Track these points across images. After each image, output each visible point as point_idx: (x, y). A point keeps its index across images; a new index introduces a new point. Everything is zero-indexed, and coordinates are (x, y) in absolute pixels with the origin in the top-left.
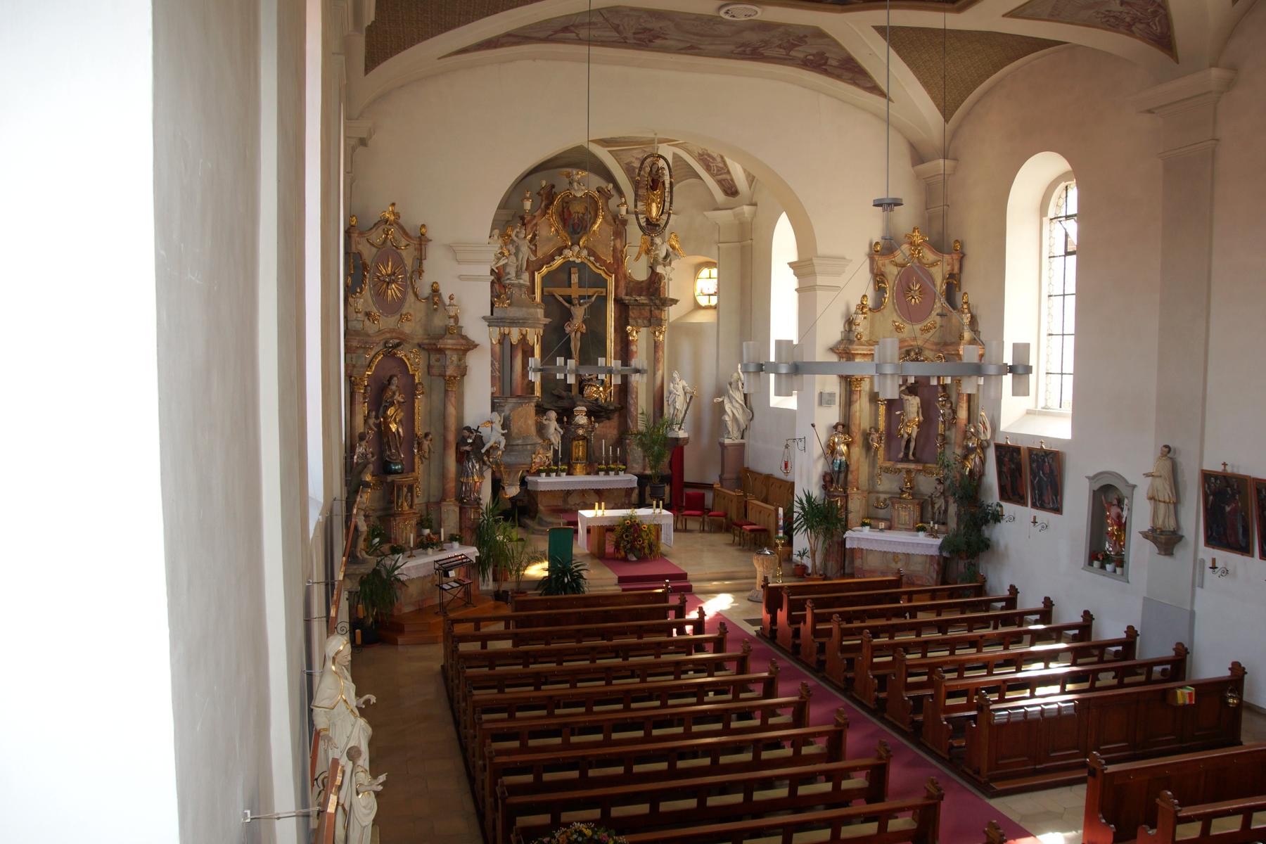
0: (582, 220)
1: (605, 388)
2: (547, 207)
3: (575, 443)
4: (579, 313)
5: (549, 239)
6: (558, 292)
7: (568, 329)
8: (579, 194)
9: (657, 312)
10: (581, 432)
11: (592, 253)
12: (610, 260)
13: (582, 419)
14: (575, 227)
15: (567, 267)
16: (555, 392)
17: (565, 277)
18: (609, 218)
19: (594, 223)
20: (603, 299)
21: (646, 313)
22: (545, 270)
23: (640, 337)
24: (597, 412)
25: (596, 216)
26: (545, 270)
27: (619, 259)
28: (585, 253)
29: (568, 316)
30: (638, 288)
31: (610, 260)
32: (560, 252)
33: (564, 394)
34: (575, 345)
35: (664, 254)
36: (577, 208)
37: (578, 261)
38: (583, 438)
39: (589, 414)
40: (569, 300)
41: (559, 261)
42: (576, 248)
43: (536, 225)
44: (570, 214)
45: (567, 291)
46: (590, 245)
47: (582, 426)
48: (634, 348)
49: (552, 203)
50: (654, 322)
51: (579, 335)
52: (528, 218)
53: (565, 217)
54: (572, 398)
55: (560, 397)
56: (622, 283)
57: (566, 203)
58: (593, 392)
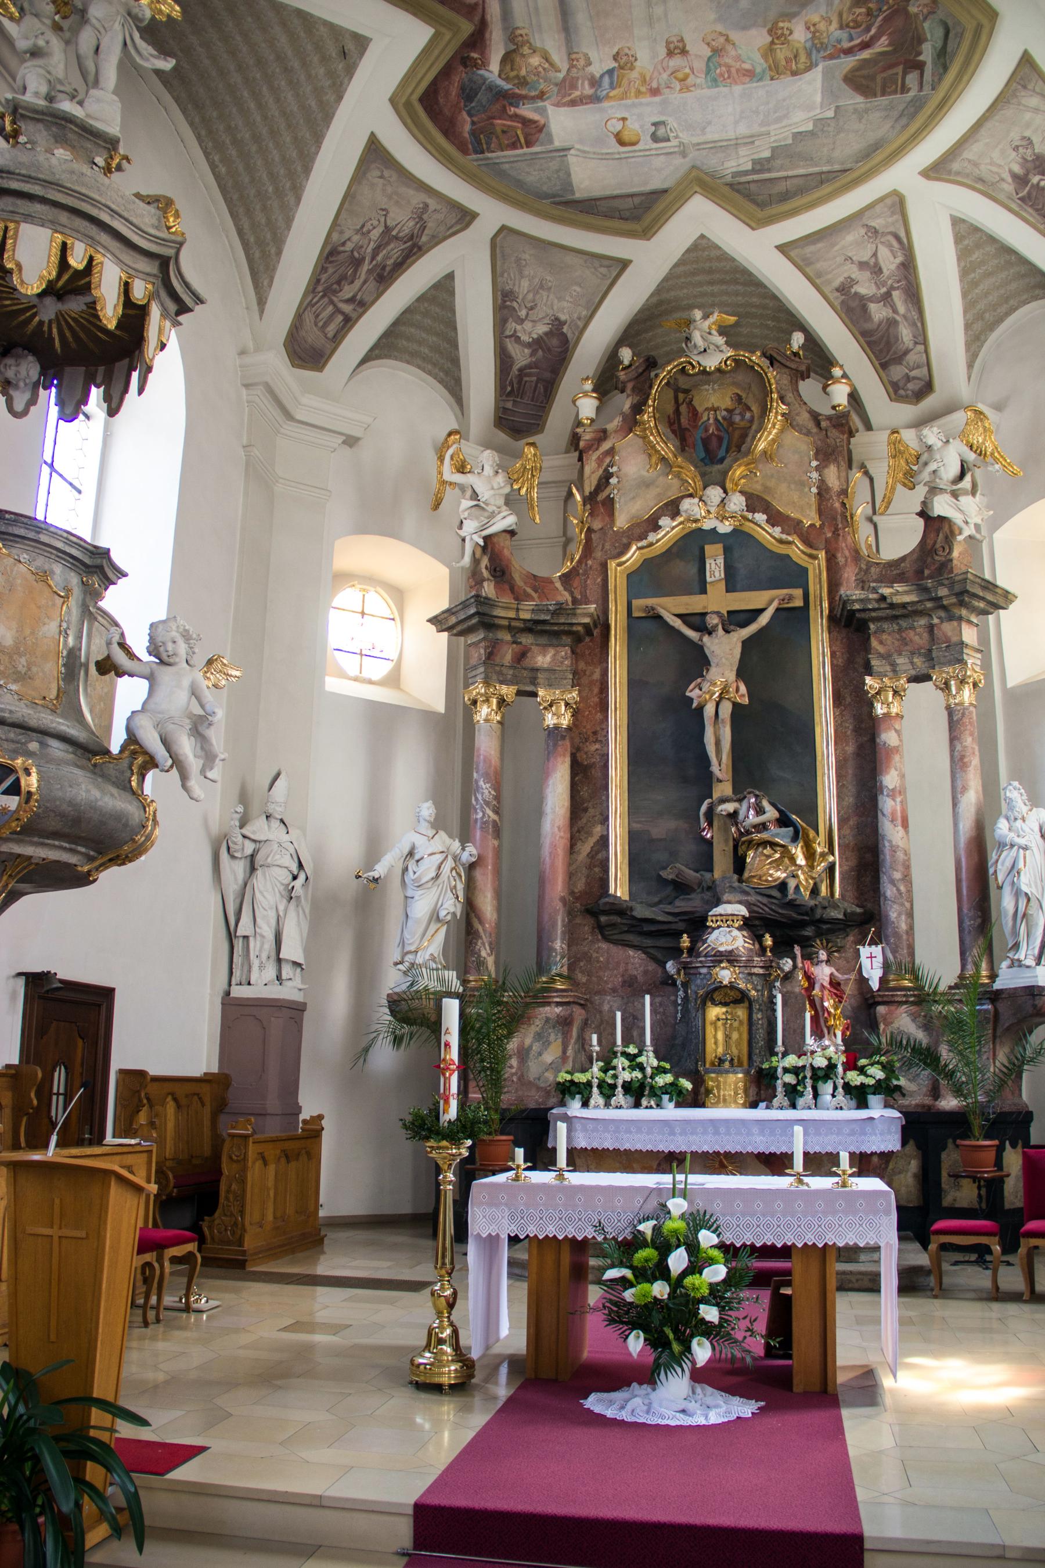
0: (727, 425)
1: (810, 855)
2: (638, 408)
3: (714, 1012)
4: (725, 650)
5: (646, 484)
6: (670, 607)
7: (693, 693)
8: (711, 362)
9: (948, 628)
10: (725, 975)
11: (755, 502)
12: (810, 518)
13: (726, 938)
14: (712, 447)
15: (695, 541)
16: (668, 874)
17: (693, 570)
18: (804, 418)
19: (761, 427)
20: (793, 619)
21: (918, 637)
22: (633, 556)
23: (914, 717)
24: (787, 926)
25: (765, 411)
26: (633, 556)
27: (834, 515)
28: (737, 502)
29: (697, 662)
30: (894, 571)
31: (810, 518)
32: (673, 508)
33: (691, 875)
34: (718, 740)
35: (954, 470)
36: (714, 400)
37: (725, 528)
38: (735, 997)
39: (752, 926)
40: (697, 621)
41: (669, 530)
42: (714, 493)
43: (611, 452)
44: (695, 414)
45: (694, 603)
46: (756, 488)
47: (730, 958)
48: (888, 737)
49: (649, 394)
50: (937, 659)
51: (726, 709)
52: (587, 436)
53: (681, 426)
54: (711, 888)
55: (681, 887)
56: (849, 575)
57: (683, 389)
58: (767, 869)
